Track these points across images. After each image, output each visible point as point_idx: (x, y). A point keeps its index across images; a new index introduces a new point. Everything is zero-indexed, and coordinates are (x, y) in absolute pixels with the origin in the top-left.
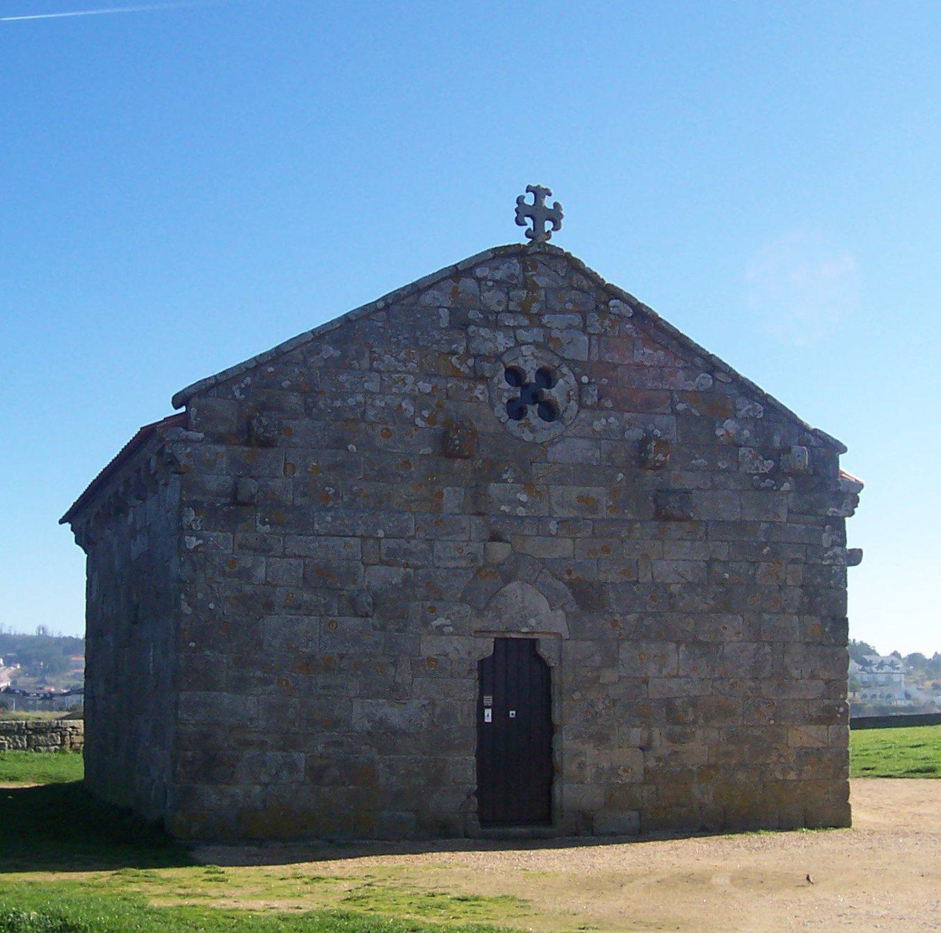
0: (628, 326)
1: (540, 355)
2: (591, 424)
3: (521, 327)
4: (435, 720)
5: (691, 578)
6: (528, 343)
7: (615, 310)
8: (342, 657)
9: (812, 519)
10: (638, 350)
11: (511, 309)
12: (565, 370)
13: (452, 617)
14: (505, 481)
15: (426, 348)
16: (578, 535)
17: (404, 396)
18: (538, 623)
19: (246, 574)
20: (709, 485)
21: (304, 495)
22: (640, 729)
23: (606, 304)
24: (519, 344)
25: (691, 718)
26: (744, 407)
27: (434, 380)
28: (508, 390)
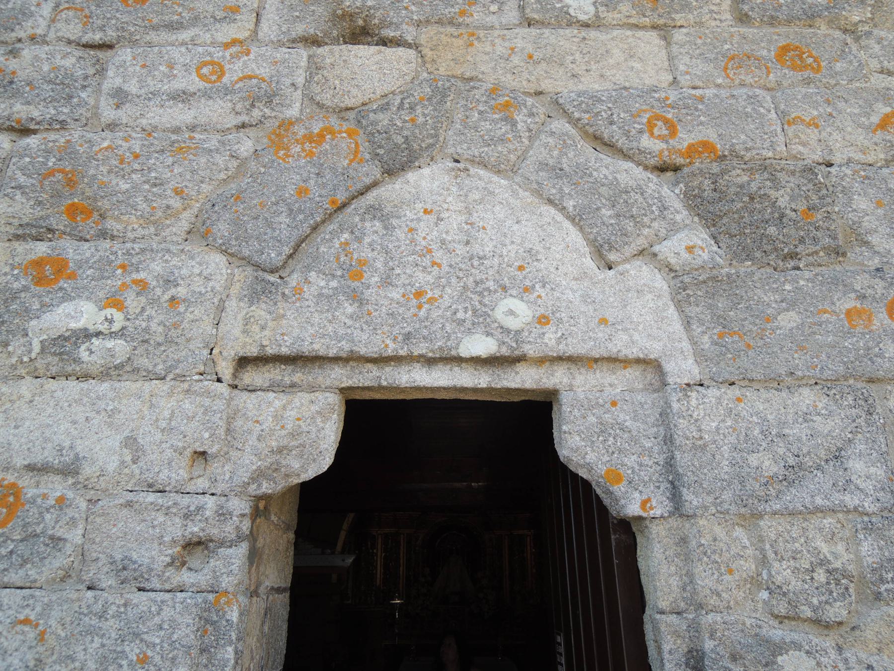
13: (133, 302)
16: (680, 19)
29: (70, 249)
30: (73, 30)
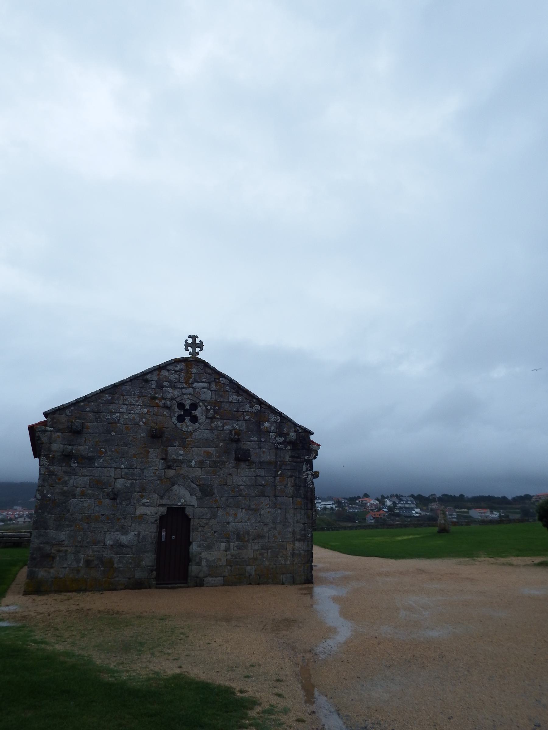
0: (227, 388)
1: (191, 398)
2: (210, 425)
3: (183, 388)
4: (140, 541)
5: (249, 483)
6: (187, 394)
7: (222, 382)
8: (103, 515)
9: (298, 460)
10: (230, 397)
11: (180, 381)
12: (201, 404)
14: (175, 446)
15: (146, 396)
17: (135, 414)
18: (185, 501)
19: (66, 483)
20: (257, 447)
21: (92, 452)
22: (225, 543)
23: (219, 379)
24: (183, 394)
25: (246, 539)
26: (273, 418)
27: (149, 408)
28: (178, 412)
29: (144, 494)
30: (139, 467)
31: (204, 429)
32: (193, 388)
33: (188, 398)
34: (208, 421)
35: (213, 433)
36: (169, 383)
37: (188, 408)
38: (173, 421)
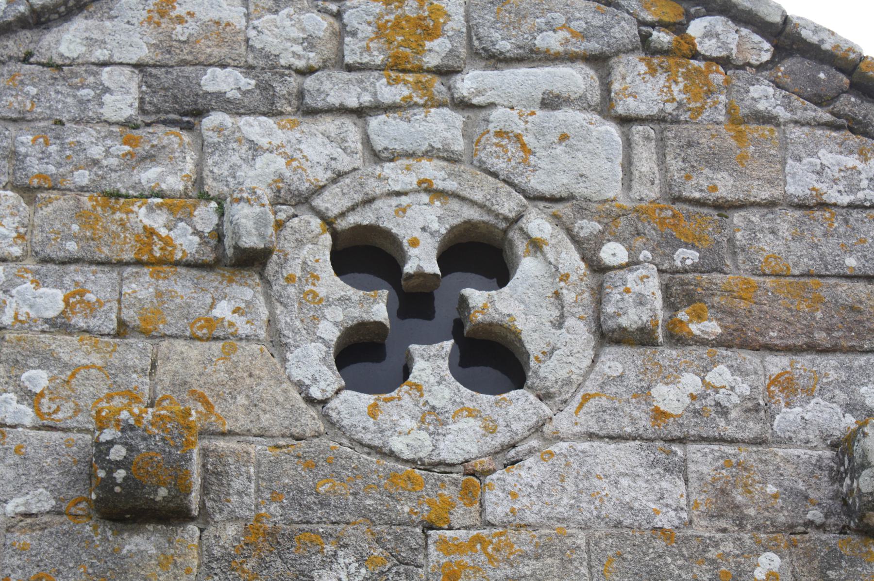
0: (756, 91)
1: (451, 185)
2: (644, 394)
7: (708, 47)
11: (349, 59)
23: (678, 28)
27: (75, 275)
28: (344, 301)
31: (591, 436)
32: (462, 105)
33: (427, 188)
34: (617, 369)
35: (682, 469)
36: (246, 75)
37: (432, 267)
38: (298, 374)
